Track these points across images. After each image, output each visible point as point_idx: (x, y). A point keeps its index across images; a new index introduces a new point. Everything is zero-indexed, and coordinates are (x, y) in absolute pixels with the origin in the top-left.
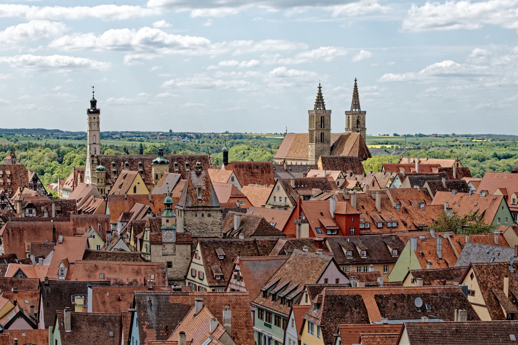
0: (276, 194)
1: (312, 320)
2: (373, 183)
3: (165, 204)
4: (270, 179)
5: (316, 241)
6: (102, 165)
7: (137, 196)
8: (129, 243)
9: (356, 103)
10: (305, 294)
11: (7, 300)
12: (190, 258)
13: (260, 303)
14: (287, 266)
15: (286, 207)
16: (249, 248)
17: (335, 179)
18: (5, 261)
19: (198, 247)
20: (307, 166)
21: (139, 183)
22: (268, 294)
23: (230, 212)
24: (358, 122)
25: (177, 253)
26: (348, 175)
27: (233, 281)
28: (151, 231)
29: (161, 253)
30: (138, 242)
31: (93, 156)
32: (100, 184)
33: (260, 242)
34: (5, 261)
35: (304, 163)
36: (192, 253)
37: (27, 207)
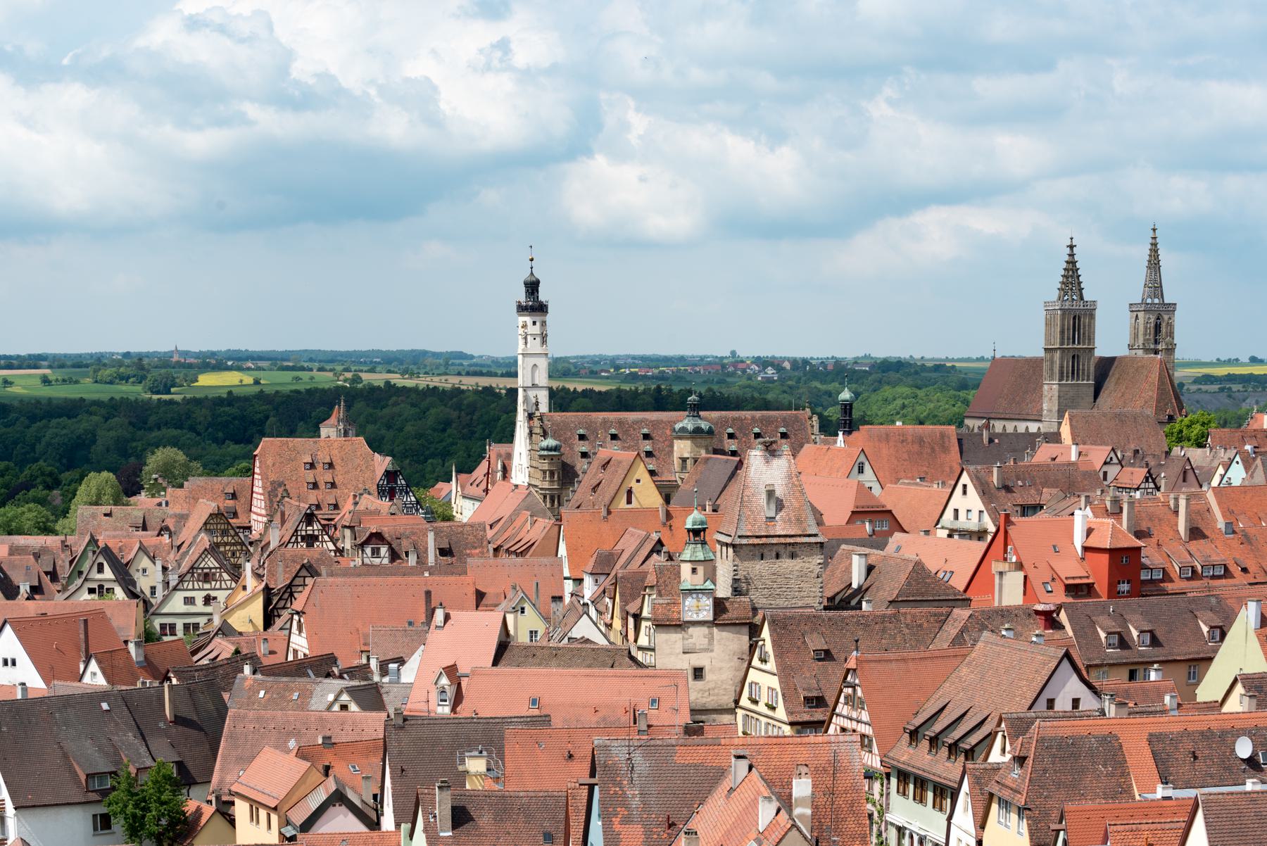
0: (957, 500)
1: (1006, 794)
2: (1185, 472)
3: (689, 530)
4: (951, 468)
5: (1037, 612)
6: (554, 437)
7: (631, 511)
8: (611, 625)
9: (1155, 286)
10: (1000, 734)
11: (309, 764)
12: (746, 658)
13: (904, 758)
14: (964, 670)
15: (980, 534)
16: (884, 630)
17: (1098, 464)
18: (310, 672)
19: (766, 633)
20: (1038, 434)
21: (638, 481)
22: (920, 735)
23: (843, 546)
24: (1157, 328)
25: (716, 647)
26: (1129, 454)
27: (842, 708)
28: (660, 594)
29: (679, 648)
30: (631, 621)
31: (530, 417)
32: (546, 485)
33: (909, 617)
34: (310, 672)
35: (1033, 427)
36: (751, 646)
37: (367, 542)
